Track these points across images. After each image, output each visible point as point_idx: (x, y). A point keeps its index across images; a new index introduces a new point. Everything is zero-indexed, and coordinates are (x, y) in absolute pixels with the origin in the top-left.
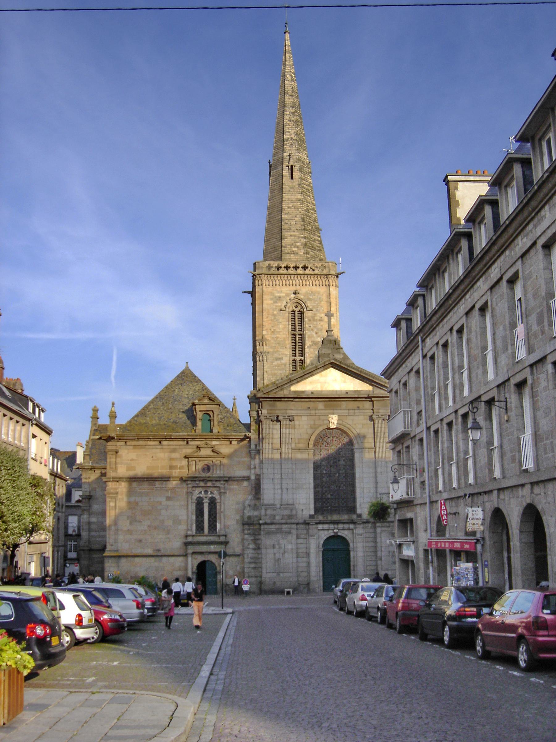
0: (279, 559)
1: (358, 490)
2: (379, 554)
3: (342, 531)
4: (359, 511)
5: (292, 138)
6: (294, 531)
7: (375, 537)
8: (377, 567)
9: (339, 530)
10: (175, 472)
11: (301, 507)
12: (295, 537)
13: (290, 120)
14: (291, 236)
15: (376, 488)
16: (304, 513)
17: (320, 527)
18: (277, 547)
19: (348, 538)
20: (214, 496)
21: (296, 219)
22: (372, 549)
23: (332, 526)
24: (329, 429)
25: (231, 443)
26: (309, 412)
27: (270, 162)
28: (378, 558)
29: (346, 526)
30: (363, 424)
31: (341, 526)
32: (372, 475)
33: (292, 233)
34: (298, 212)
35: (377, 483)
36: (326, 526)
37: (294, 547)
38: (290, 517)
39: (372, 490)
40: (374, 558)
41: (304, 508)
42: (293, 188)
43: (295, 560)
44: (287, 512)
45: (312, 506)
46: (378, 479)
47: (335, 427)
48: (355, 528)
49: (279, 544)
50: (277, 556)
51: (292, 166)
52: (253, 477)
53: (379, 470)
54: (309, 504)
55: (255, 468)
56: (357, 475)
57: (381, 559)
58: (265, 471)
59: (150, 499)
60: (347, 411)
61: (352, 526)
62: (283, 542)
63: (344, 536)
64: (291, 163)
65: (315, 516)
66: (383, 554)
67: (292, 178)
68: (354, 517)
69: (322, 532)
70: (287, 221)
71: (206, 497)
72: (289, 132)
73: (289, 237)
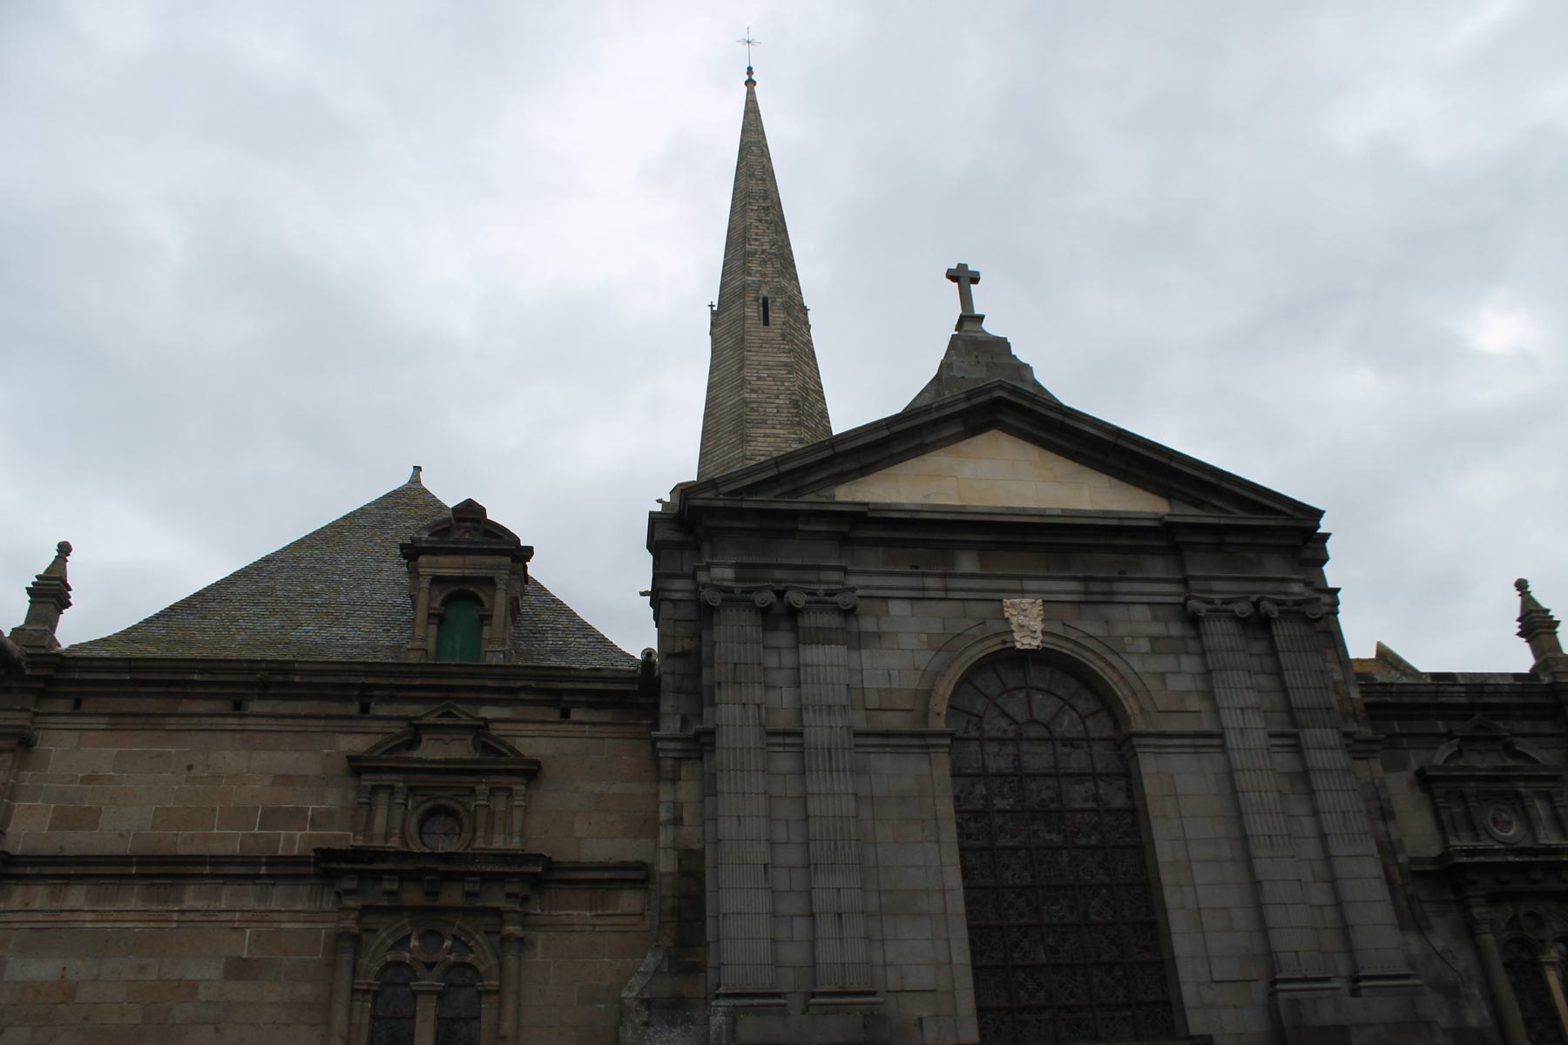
1: (1178, 924)
5: (764, 251)
10: (290, 840)
13: (760, 220)
14: (766, 436)
15: (1259, 906)
20: (470, 958)
21: (777, 401)
25: (565, 714)
27: (712, 306)
30: (1153, 639)
33: (768, 431)
34: (783, 388)
35: (1255, 884)
42: (766, 341)
46: (1263, 867)
47: (1036, 643)
51: (765, 300)
52: (666, 864)
54: (952, 992)
55: (677, 821)
56: (1165, 851)
58: (727, 828)
59: (142, 969)
64: (764, 292)
67: (766, 322)
70: (755, 405)
71: (430, 966)
72: (756, 240)
73: (762, 439)
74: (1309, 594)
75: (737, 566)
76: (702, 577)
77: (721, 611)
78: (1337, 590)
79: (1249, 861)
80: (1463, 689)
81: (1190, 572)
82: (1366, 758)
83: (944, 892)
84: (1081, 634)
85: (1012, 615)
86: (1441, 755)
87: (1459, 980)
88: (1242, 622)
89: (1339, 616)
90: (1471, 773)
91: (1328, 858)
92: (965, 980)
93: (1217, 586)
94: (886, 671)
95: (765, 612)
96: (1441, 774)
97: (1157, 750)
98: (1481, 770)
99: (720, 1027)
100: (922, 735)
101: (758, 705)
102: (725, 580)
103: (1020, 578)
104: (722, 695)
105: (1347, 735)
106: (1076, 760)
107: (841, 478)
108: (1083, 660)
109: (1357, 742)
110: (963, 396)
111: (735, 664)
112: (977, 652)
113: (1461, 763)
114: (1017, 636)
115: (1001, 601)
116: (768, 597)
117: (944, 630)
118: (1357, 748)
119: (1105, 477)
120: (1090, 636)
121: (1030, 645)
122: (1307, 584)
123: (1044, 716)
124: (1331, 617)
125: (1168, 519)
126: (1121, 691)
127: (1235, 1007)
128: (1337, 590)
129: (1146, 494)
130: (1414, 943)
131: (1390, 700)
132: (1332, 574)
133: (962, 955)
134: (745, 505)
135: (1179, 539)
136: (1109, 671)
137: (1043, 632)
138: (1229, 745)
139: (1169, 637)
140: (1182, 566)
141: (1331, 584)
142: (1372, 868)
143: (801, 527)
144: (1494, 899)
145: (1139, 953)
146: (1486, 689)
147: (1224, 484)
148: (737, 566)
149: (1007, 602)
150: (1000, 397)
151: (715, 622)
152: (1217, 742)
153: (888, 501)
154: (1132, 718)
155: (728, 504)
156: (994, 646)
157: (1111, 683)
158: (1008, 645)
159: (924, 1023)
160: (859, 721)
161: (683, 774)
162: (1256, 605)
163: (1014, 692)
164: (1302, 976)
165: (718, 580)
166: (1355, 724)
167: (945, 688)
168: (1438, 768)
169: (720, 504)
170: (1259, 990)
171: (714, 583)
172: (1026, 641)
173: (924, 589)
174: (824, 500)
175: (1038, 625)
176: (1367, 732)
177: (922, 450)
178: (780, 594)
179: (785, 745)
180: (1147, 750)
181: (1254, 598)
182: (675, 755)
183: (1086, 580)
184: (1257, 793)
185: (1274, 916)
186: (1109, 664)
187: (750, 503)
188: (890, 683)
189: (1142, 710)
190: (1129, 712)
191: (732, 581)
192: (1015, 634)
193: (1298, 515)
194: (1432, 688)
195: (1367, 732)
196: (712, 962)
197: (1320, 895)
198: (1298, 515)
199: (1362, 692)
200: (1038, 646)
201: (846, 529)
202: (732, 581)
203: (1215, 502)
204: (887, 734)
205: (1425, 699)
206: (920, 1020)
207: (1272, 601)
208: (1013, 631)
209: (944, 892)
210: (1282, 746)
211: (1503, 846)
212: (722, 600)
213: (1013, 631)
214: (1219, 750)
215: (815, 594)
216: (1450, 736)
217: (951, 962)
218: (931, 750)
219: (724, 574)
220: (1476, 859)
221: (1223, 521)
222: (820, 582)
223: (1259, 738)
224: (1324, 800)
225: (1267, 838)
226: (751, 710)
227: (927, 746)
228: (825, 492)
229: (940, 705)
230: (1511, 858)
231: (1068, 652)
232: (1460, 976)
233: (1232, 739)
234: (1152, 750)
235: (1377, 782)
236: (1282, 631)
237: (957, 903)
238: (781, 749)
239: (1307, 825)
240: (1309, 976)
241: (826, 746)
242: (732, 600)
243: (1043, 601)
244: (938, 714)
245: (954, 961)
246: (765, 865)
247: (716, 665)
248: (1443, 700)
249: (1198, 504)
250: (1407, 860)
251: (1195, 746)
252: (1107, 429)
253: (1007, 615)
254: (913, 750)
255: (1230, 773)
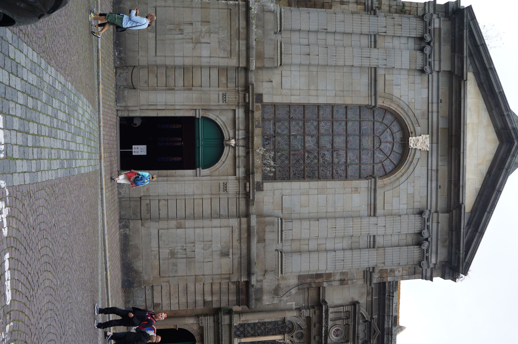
0: (181, 32)
2: (189, 223)
3: (231, 154)
4: (267, 186)
6: (233, 62)
7: (220, 217)
8: (163, 219)
9: (234, 148)
11: (276, 79)
12: (223, 62)
15: (309, 219)
16: (265, 84)
17: (240, 113)
18: (205, 29)
19: (217, 165)
22: (198, 210)
23: (241, 134)
24: (406, 135)
26: (435, 100)
28: (183, 221)
29: (241, 162)
31: (241, 151)
32: (330, 209)
36: (241, 124)
37: (205, 61)
38: (260, 56)
39: (305, 211)
40: (181, 213)
41: (274, 83)
43: (179, 62)
44: (269, 51)
45: (277, 99)
46: (323, 222)
47: (411, 145)
48: (238, 179)
49: (209, 32)
50: (188, 29)
53: (340, 223)
56: (330, 184)
57: (179, 227)
58: (340, 16)
60: (434, 168)
61: (241, 172)
62: (214, 38)
63: (223, 158)
65: (260, 105)
66: (190, 232)
68: (258, 178)
69: (230, 115)
74: (431, 266)
75: (440, 29)
76: (435, 16)
77: (422, 22)
78: (432, 280)
79: (327, 218)
80: (390, 326)
81: (440, 215)
82: (364, 278)
83: (317, 96)
84: (415, 165)
85: (422, 137)
86: (363, 311)
87: (279, 296)
88: (420, 234)
89: (421, 279)
90: (357, 323)
91: (326, 251)
92: (286, 100)
93: (435, 225)
94: (399, 84)
95: (422, 39)
96: (357, 311)
97: (369, 189)
98: (358, 327)
99: (270, 7)
100: (375, 95)
101: (386, 32)
102: (434, 24)
103: (437, 143)
104: (390, 21)
105: (373, 268)
106: (366, 158)
107: (477, 75)
108: (405, 164)
109: (371, 273)
110: (515, 126)
111: (401, 25)
112: (408, 122)
113: (361, 321)
114: (414, 138)
115: (428, 134)
116: (428, 39)
117: (417, 109)
118: (368, 274)
119: (480, 187)
120: (414, 169)
121: (411, 143)
122: (435, 264)
123: (382, 146)
124: (421, 276)
125: (463, 206)
126: (392, 177)
127: (273, 202)
128: (432, 280)
129: (473, 203)
130: (294, 281)
131: (387, 294)
132: (437, 280)
133: (294, 100)
134: (465, 31)
135: (454, 211)
136: (401, 174)
137: (416, 149)
138: (371, 218)
139: (414, 202)
140: (443, 212)
141: (434, 279)
142: (322, 269)
143: (456, 55)
144: (309, 319)
145: (293, 171)
146: (390, 337)
147: (478, 234)
148: (440, 29)
149: (428, 136)
150: (514, 143)
151: (417, 19)
152: (372, 214)
153: (468, 93)
154: (382, 180)
155: (465, 24)
156: (410, 128)
157: (396, 174)
158: (411, 135)
159: (271, 83)
160: (380, 72)
161: (359, 6)
162: (427, 240)
163: (392, 136)
164: (283, 230)
165: (434, 21)
166: (378, 277)
167: (393, 107)
168: (359, 310)
169: (465, 21)
170: (278, 213)
171: (433, 20)
172: (412, 141)
173: (432, 103)
174: (468, 67)
175: (419, 147)
176: (375, 281)
177: (490, 110)
178: (429, 44)
179: (371, 42)
180: (369, 184)
181: (429, 239)
182: (366, 4)
183: (437, 170)
184: (352, 226)
185: (305, 224)
186: (403, 174)
187: (466, 33)
188: (395, 85)
189: (385, 185)
190: (384, 180)
191: (434, 27)
192: (415, 137)
193: (464, 264)
194: (391, 314)
195: (375, 281)
196: (292, 8)
197: (313, 245)
198: (464, 264)
199: (390, 282)
200: (410, 146)
201: (456, 73)
202: (434, 27)
203: (470, 231)
204: (375, 81)
205: (386, 310)
206: (272, 81)
207: (428, 247)
208: (416, 137)
209: (317, 96)
210: (370, 241)
211: (328, 331)
212: (426, 21)
213: (416, 137)
214: (369, 215)
215: (429, 58)
216: (372, 318)
217: (291, 95)
218: (370, 98)
219: (436, 24)
220: (324, 314)
221: (462, 230)
222: (434, 61)
223: (373, 231)
224: (348, 253)
225: (335, 227)
226: (384, 30)
227: (371, 96)
228: (471, 67)
229: (387, 104)
230: (324, 329)
231: (408, 159)
232: (281, 297)
233: (373, 220)
234: (369, 187)
235: (355, 280)
236: (415, 251)
237: (313, 100)
238: (369, 41)
239: (339, 246)
240: (283, 232)
241: (371, 56)
242: (426, 25)
243: (428, 151)
244: (383, 102)
245: (292, 96)
246: (327, 29)
247: (401, 18)
248: (386, 318)
249: (469, 224)
250: (324, 286)
251: (371, 205)
252: (501, 187)
253: (422, 135)
254: (370, 91)
255: (361, 217)
